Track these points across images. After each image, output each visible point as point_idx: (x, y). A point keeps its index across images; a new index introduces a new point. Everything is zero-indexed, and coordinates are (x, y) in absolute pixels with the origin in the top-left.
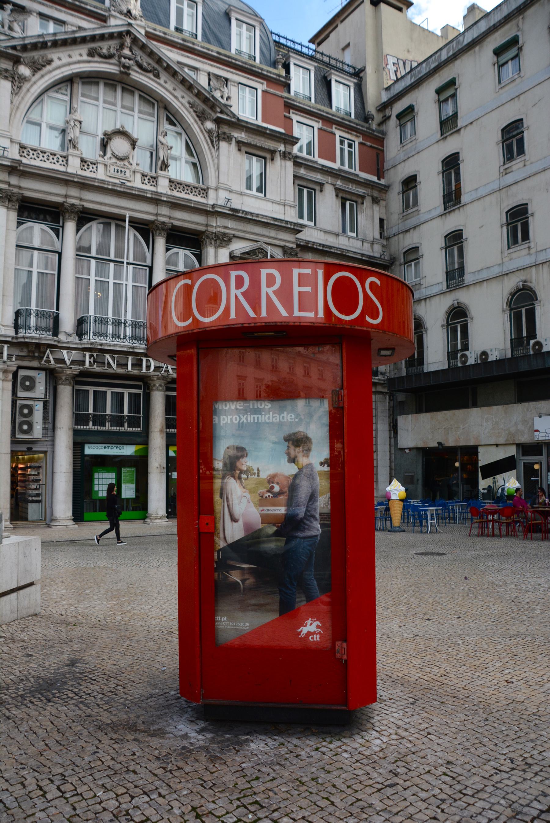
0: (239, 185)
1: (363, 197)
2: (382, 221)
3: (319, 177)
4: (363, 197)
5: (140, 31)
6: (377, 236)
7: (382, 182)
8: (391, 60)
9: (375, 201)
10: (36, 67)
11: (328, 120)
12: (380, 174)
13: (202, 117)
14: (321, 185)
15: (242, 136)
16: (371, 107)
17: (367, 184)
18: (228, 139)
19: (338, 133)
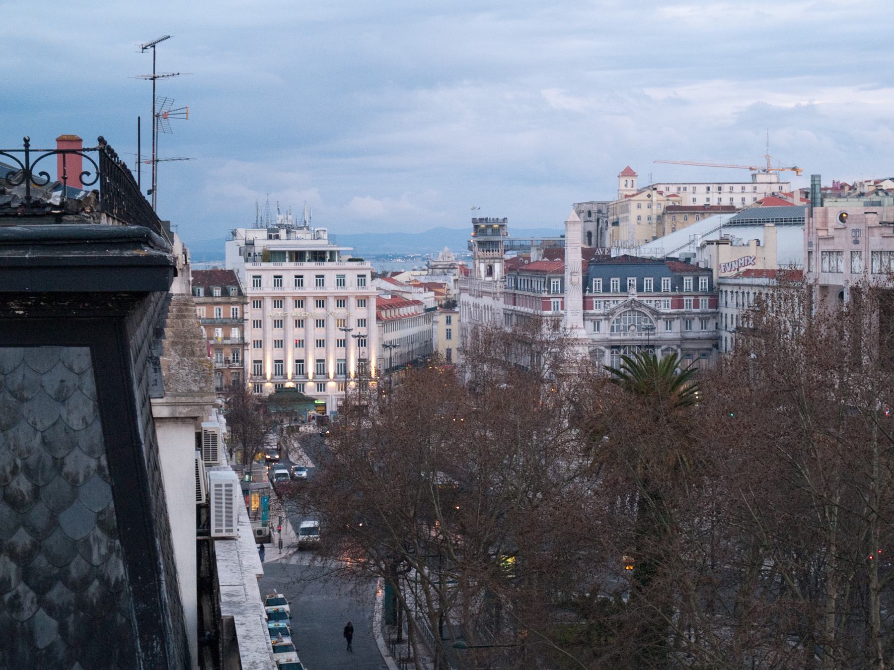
0: (664, 330)
1: (709, 318)
2: (717, 324)
3: (693, 316)
4: (709, 318)
5: (637, 299)
6: (715, 329)
7: (718, 310)
8: (722, 265)
9: (714, 318)
10: (612, 314)
11: (696, 296)
12: (717, 307)
13: (653, 314)
14: (694, 319)
15: (664, 317)
16: (715, 284)
17: (712, 313)
18: (660, 319)
19: (700, 298)
